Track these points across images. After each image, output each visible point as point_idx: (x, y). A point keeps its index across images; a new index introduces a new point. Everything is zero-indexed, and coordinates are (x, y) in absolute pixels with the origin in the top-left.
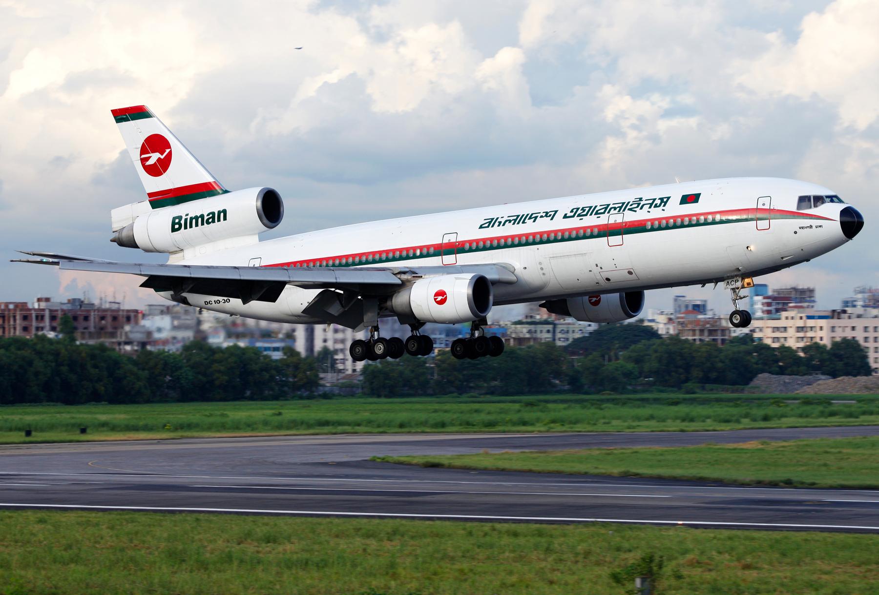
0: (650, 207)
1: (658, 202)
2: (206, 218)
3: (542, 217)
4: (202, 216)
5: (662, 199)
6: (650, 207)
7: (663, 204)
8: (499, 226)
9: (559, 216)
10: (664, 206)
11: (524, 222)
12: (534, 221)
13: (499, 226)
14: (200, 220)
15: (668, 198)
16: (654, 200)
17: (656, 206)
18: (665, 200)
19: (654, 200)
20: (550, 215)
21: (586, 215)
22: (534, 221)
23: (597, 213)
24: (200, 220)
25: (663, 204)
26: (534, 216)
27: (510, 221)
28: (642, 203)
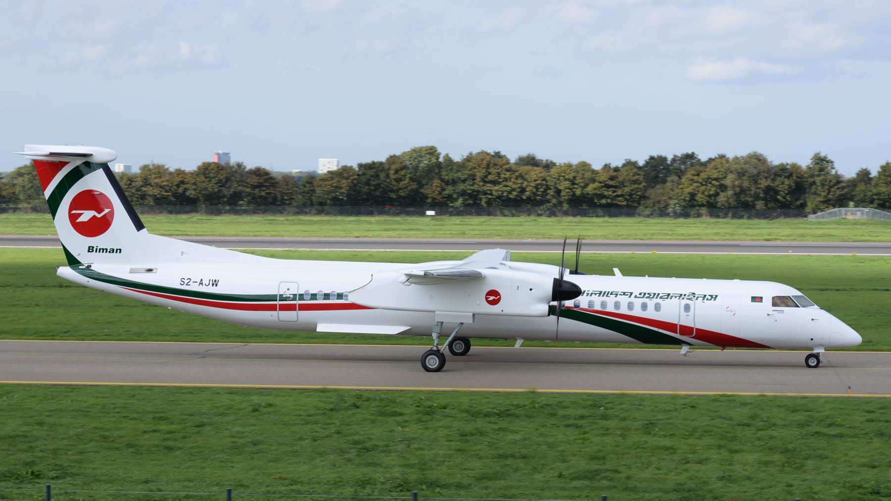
0: (703, 299)
1: (710, 298)
2: (108, 250)
3: (620, 295)
4: (107, 249)
5: (712, 296)
6: (703, 299)
7: (713, 299)
8: (587, 295)
9: (633, 296)
10: (715, 300)
11: (607, 296)
12: (616, 296)
13: (587, 295)
14: (105, 251)
15: (716, 296)
16: (705, 296)
17: (707, 299)
18: (714, 296)
19: (705, 296)
20: (628, 295)
21: (653, 298)
22: (616, 296)
23: (661, 298)
24: (105, 251)
25: (713, 299)
26: (613, 293)
27: (596, 294)
28: (696, 296)
